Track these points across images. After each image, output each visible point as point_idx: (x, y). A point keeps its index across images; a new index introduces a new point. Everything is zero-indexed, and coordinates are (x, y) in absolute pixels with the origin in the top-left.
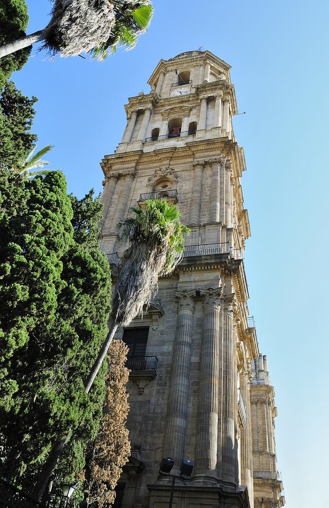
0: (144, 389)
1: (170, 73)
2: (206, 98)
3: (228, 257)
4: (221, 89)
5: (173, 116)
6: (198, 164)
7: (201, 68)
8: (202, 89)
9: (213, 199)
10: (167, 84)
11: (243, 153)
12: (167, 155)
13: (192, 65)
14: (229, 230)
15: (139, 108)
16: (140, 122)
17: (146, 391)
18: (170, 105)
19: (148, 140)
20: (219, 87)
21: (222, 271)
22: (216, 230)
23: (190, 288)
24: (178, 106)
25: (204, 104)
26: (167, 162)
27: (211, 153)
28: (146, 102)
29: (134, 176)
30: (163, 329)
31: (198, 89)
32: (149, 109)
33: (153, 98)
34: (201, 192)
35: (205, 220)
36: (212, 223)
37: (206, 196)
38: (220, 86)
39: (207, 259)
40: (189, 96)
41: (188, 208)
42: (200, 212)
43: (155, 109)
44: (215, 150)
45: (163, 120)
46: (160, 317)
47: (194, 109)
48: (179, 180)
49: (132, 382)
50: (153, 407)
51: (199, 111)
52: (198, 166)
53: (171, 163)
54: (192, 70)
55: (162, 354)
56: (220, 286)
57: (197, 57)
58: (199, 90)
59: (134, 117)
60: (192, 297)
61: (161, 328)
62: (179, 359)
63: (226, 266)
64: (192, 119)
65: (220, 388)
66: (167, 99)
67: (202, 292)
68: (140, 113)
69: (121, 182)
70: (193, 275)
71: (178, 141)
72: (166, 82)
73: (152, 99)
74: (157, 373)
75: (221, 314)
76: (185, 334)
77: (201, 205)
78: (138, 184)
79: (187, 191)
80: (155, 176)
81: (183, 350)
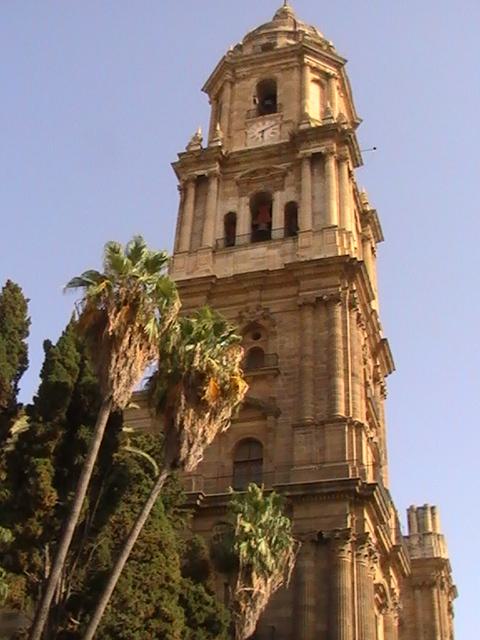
2: (308, 158)
3: (357, 484)
4: (332, 137)
5: (260, 187)
6: (304, 304)
7: (295, 75)
9: (330, 374)
13: (278, 65)
14: (360, 426)
19: (221, 244)
26: (255, 294)
31: (293, 137)
35: (322, 415)
40: (279, 146)
47: (290, 173)
51: (299, 178)
52: (306, 308)
53: (264, 296)
54: (279, 75)
56: (349, 526)
59: (191, 192)
60: (313, 541)
66: (242, 152)
68: (201, 182)
71: (269, 248)
72: (236, 103)
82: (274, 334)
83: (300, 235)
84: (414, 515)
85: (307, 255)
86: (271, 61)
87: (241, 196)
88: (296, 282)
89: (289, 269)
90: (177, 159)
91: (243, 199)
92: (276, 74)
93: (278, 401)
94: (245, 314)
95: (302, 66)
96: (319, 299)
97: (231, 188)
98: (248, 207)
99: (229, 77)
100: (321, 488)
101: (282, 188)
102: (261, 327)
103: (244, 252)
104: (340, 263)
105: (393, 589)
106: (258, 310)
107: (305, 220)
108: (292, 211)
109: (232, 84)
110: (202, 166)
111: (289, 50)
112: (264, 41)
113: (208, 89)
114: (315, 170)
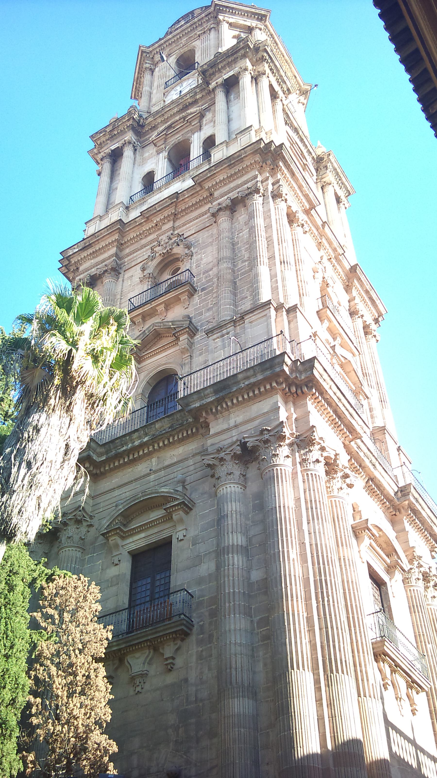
0: (173, 658)
6: (220, 210)
8: (211, 71)
10: (158, 86)
11: (337, 161)
12: (166, 213)
13: (196, 34)
15: (113, 148)
17: (179, 662)
18: (165, 121)
20: (239, 54)
22: (264, 318)
23: (230, 441)
24: (177, 118)
27: (239, 181)
28: (122, 133)
30: (196, 532)
32: (130, 143)
33: (131, 120)
34: (233, 260)
38: (242, 52)
39: (248, 378)
41: (215, 295)
42: (235, 295)
43: (142, 139)
44: (247, 173)
45: (158, 153)
46: (187, 513)
47: (207, 113)
49: (152, 651)
50: (194, 689)
52: (221, 213)
53: (177, 224)
55: (200, 581)
58: (208, 74)
59: (107, 166)
60: (235, 457)
61: (192, 533)
62: (224, 582)
63: (287, 378)
64: (206, 132)
65: (309, 620)
70: (232, 415)
72: (156, 84)
73: (131, 122)
74: (195, 620)
75: (294, 474)
76: (230, 530)
77: (235, 283)
78: (127, 283)
79: (210, 266)
80: (153, 258)
81: (231, 562)
90: (91, 145)
91: (161, 155)
94: (157, 249)
95: (218, 23)
97: (151, 150)
98: (166, 160)
99: (148, 65)
100: (238, 383)
104: (255, 153)
110: (115, 142)
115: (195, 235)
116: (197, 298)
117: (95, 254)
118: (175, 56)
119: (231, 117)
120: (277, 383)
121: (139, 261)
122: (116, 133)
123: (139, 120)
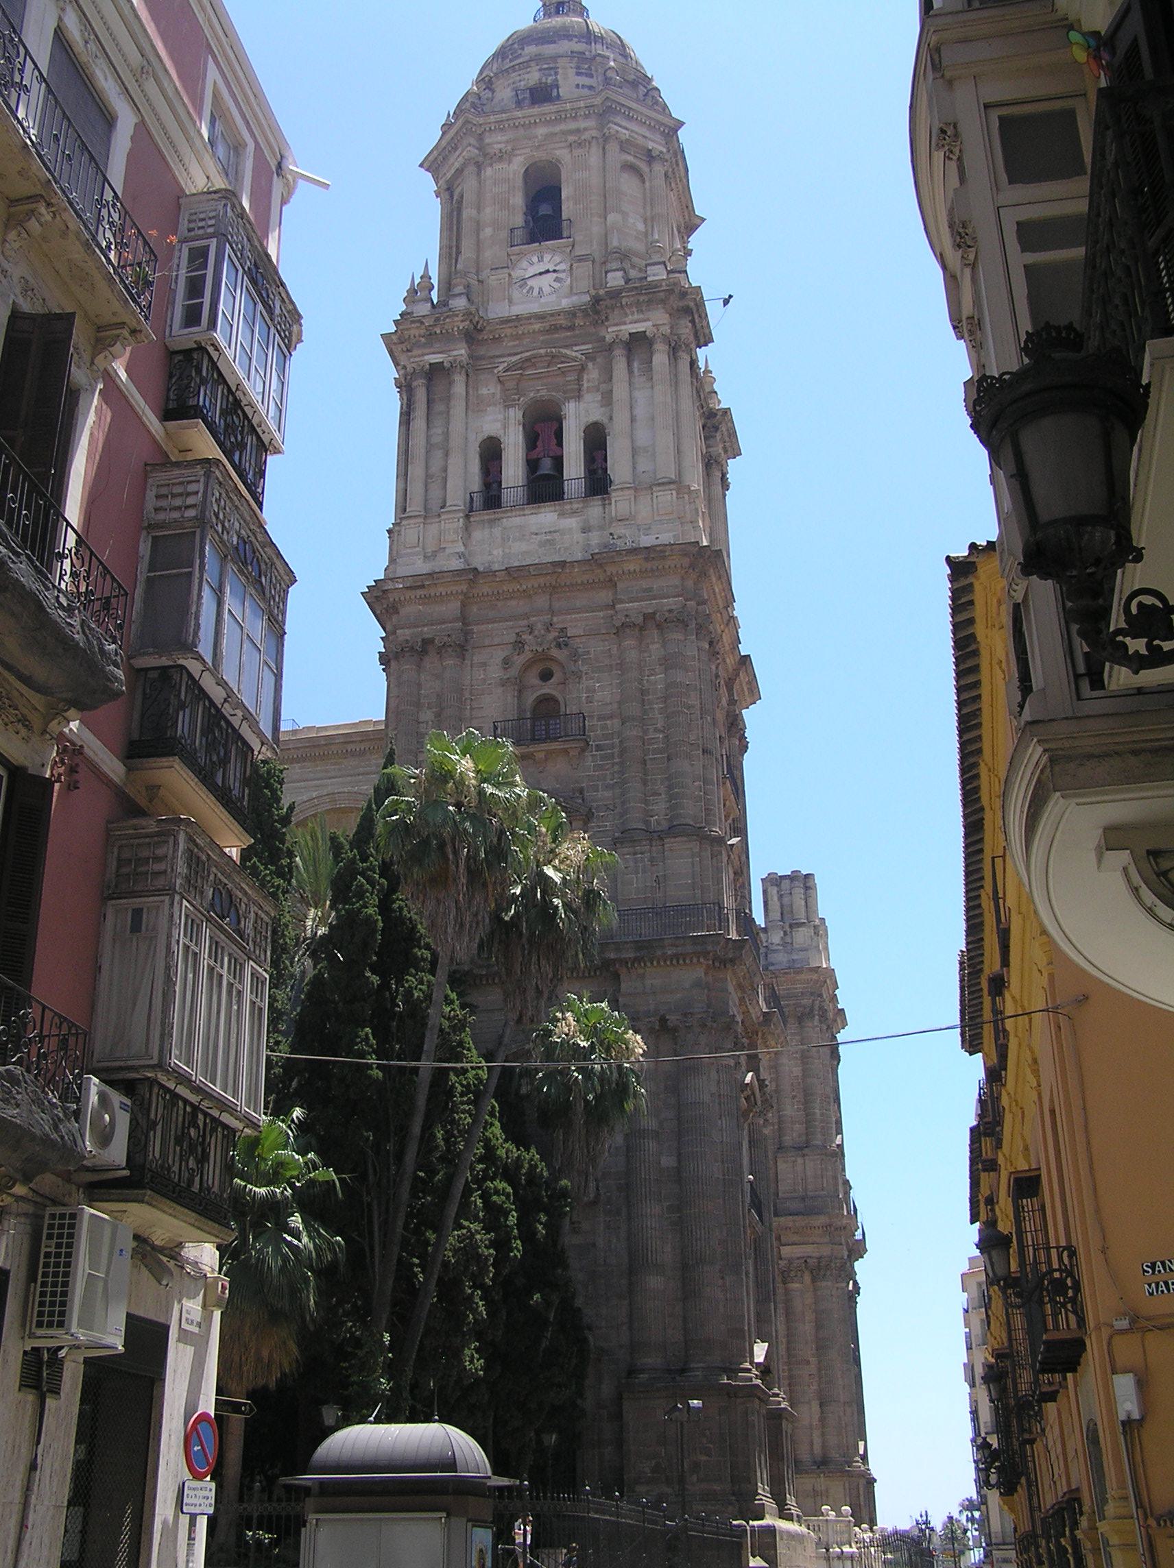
1: (498, 166)
4: (663, 302)
5: (538, 391)
7: (594, 157)
12: (542, 580)
13: (564, 133)
16: (439, 407)
21: (708, 966)
25: (619, 354)
26: (542, 601)
28: (447, 337)
29: (462, 647)
31: (597, 300)
32: (462, 367)
35: (659, 819)
36: (673, 830)
37: (656, 730)
40: (571, 313)
48: (584, 669)
54: (563, 154)
57: (576, 105)
59: (421, 395)
66: (506, 321)
67: (673, 1019)
69: (431, 662)
72: (488, 212)
77: (644, 762)
82: (578, 675)
83: (613, 494)
84: (773, 891)
85: (627, 536)
86: (548, 123)
87: (507, 407)
88: (611, 583)
89: (594, 561)
92: (558, 152)
93: (586, 794)
94: (526, 637)
96: (649, 617)
98: (521, 428)
101: (579, 397)
102: (552, 659)
103: (517, 521)
105: (764, 1080)
106: (548, 630)
107: (618, 466)
108: (596, 440)
109: (479, 166)
111: (582, 104)
112: (533, 77)
113: (433, 164)
114: (636, 364)
115: (584, 639)
116: (590, 758)
117: (426, 600)
118: (521, 159)
119: (635, 413)
120: (705, 957)
121: (497, 640)
122: (438, 332)
123: (478, 322)
